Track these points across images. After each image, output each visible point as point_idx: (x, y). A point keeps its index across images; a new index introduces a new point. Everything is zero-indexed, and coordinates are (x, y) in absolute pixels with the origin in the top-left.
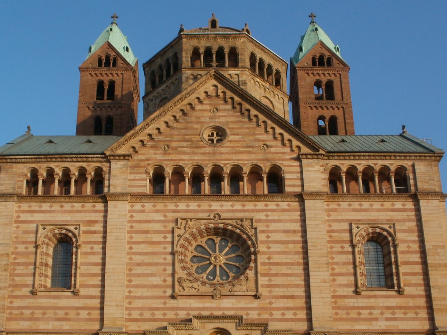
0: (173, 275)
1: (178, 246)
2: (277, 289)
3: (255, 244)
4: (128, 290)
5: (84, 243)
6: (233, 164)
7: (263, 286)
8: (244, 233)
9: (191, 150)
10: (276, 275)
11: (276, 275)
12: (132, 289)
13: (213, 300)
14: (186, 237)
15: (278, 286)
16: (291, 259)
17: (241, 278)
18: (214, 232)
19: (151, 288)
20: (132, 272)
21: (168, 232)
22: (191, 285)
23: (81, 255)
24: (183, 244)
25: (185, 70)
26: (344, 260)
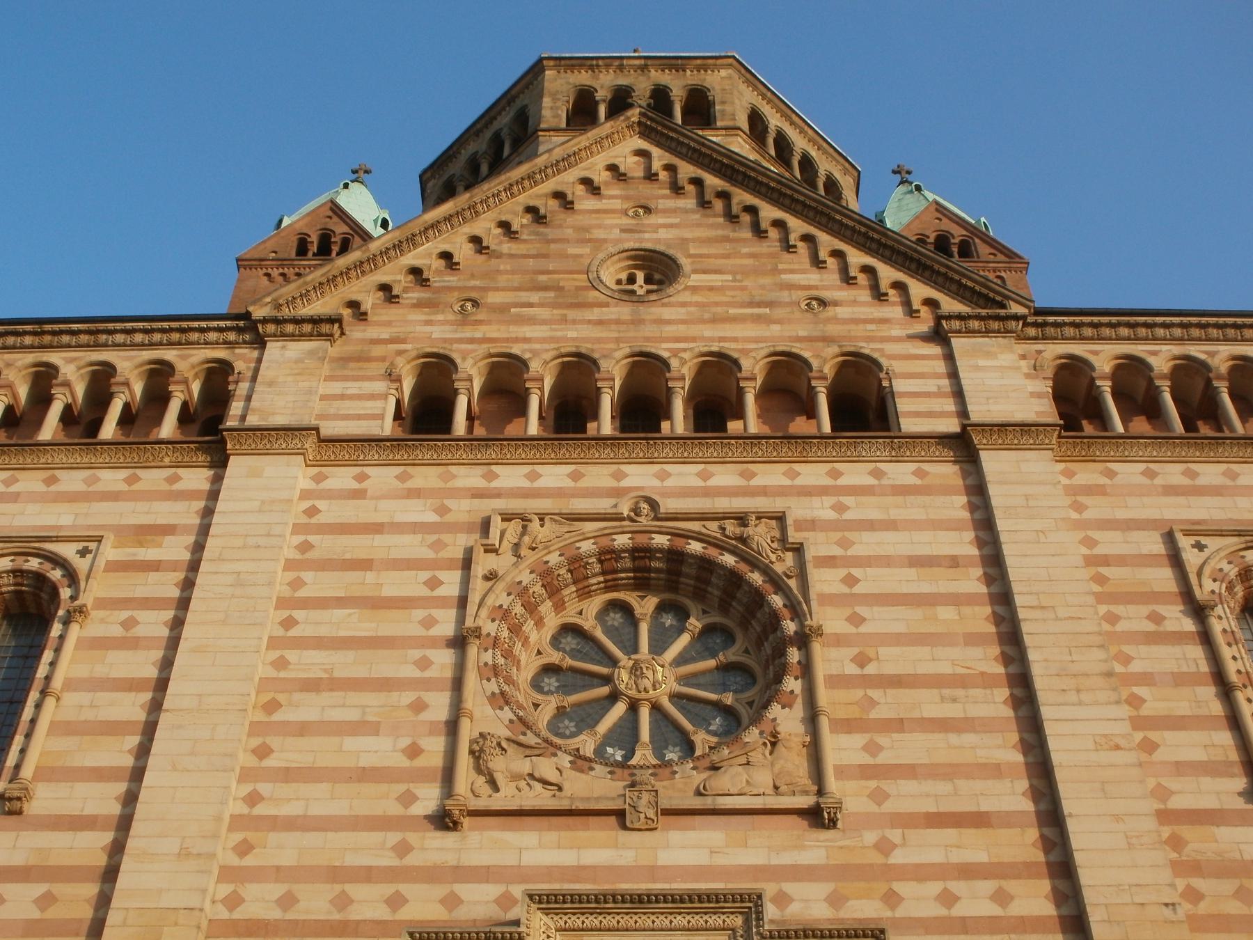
0: (452, 728)
1: (484, 613)
2: (908, 786)
3: (799, 603)
4: (246, 789)
5: (102, 603)
6: (706, 349)
7: (841, 772)
8: (754, 564)
9: (555, 312)
10: (898, 725)
11: (898, 725)
12: (264, 788)
13: (624, 836)
14: (520, 582)
15: (909, 771)
16: (954, 663)
17: (747, 740)
18: (634, 570)
19: (350, 780)
20: (278, 717)
21: (448, 565)
22: (525, 766)
23: (77, 648)
24: (505, 607)
25: (547, 134)
26: (1171, 666)
